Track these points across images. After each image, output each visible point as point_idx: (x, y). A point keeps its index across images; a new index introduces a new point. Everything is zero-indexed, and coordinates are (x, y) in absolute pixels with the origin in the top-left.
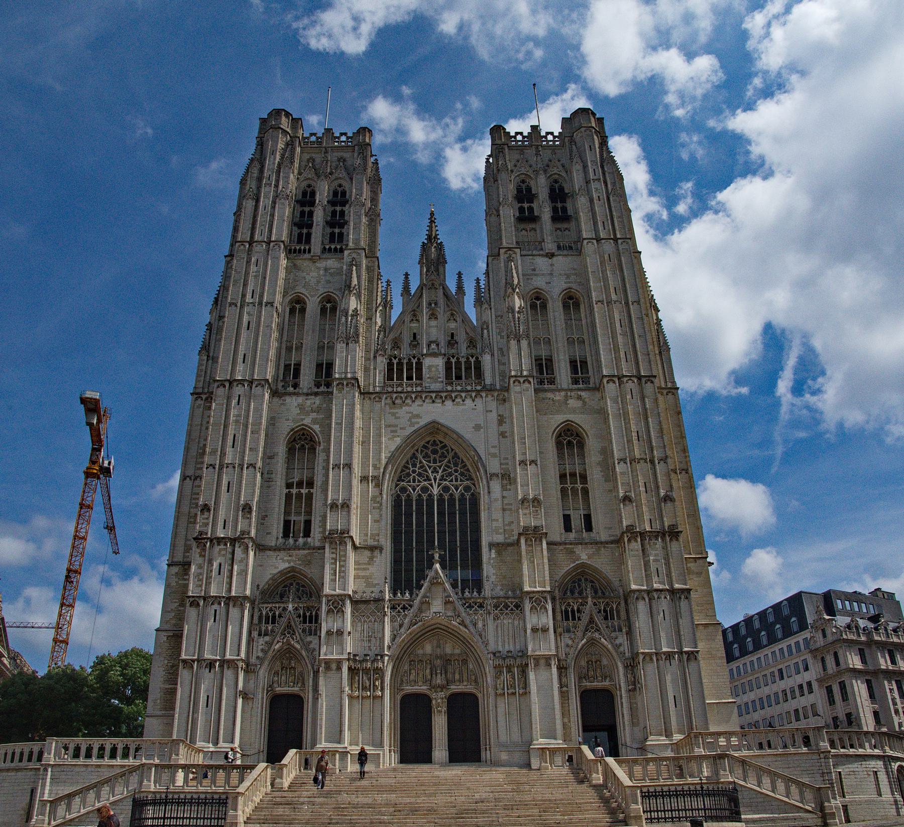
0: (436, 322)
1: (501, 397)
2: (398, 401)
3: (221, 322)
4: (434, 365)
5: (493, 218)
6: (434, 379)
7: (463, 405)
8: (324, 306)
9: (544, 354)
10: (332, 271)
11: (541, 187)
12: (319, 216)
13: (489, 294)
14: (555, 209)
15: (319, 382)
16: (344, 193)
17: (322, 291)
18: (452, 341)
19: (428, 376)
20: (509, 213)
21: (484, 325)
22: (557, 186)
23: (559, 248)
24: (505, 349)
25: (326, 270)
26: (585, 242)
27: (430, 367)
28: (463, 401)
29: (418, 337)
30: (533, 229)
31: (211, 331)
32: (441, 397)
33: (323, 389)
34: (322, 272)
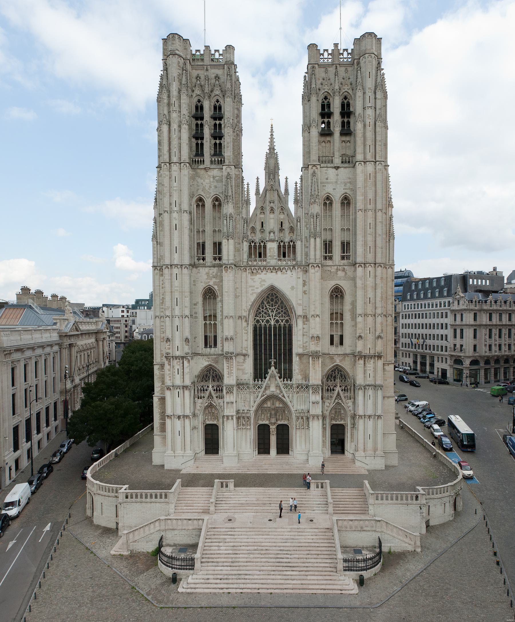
0: (273, 215)
1: (305, 269)
2: (255, 271)
3: (160, 217)
4: (272, 248)
5: (306, 134)
6: (272, 257)
7: (286, 274)
8: (215, 203)
9: (328, 238)
10: (217, 178)
11: (336, 108)
12: (207, 132)
13: (302, 196)
14: (343, 123)
15: (215, 257)
16: (220, 108)
17: (212, 194)
18: (281, 230)
19: (269, 255)
20: (315, 132)
21: (298, 220)
22: (346, 102)
23: (342, 162)
24: (308, 238)
25: (214, 177)
26: (357, 163)
27: (270, 249)
28: (286, 271)
29: (264, 225)
30: (329, 141)
31: (156, 223)
32: (276, 269)
33: (217, 262)
34: (212, 179)
